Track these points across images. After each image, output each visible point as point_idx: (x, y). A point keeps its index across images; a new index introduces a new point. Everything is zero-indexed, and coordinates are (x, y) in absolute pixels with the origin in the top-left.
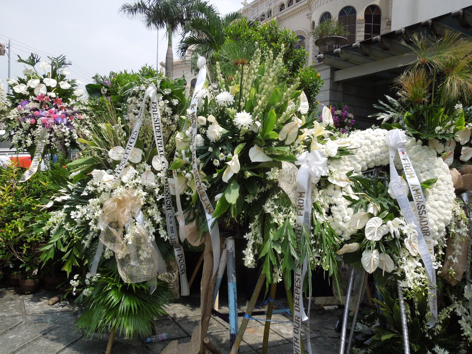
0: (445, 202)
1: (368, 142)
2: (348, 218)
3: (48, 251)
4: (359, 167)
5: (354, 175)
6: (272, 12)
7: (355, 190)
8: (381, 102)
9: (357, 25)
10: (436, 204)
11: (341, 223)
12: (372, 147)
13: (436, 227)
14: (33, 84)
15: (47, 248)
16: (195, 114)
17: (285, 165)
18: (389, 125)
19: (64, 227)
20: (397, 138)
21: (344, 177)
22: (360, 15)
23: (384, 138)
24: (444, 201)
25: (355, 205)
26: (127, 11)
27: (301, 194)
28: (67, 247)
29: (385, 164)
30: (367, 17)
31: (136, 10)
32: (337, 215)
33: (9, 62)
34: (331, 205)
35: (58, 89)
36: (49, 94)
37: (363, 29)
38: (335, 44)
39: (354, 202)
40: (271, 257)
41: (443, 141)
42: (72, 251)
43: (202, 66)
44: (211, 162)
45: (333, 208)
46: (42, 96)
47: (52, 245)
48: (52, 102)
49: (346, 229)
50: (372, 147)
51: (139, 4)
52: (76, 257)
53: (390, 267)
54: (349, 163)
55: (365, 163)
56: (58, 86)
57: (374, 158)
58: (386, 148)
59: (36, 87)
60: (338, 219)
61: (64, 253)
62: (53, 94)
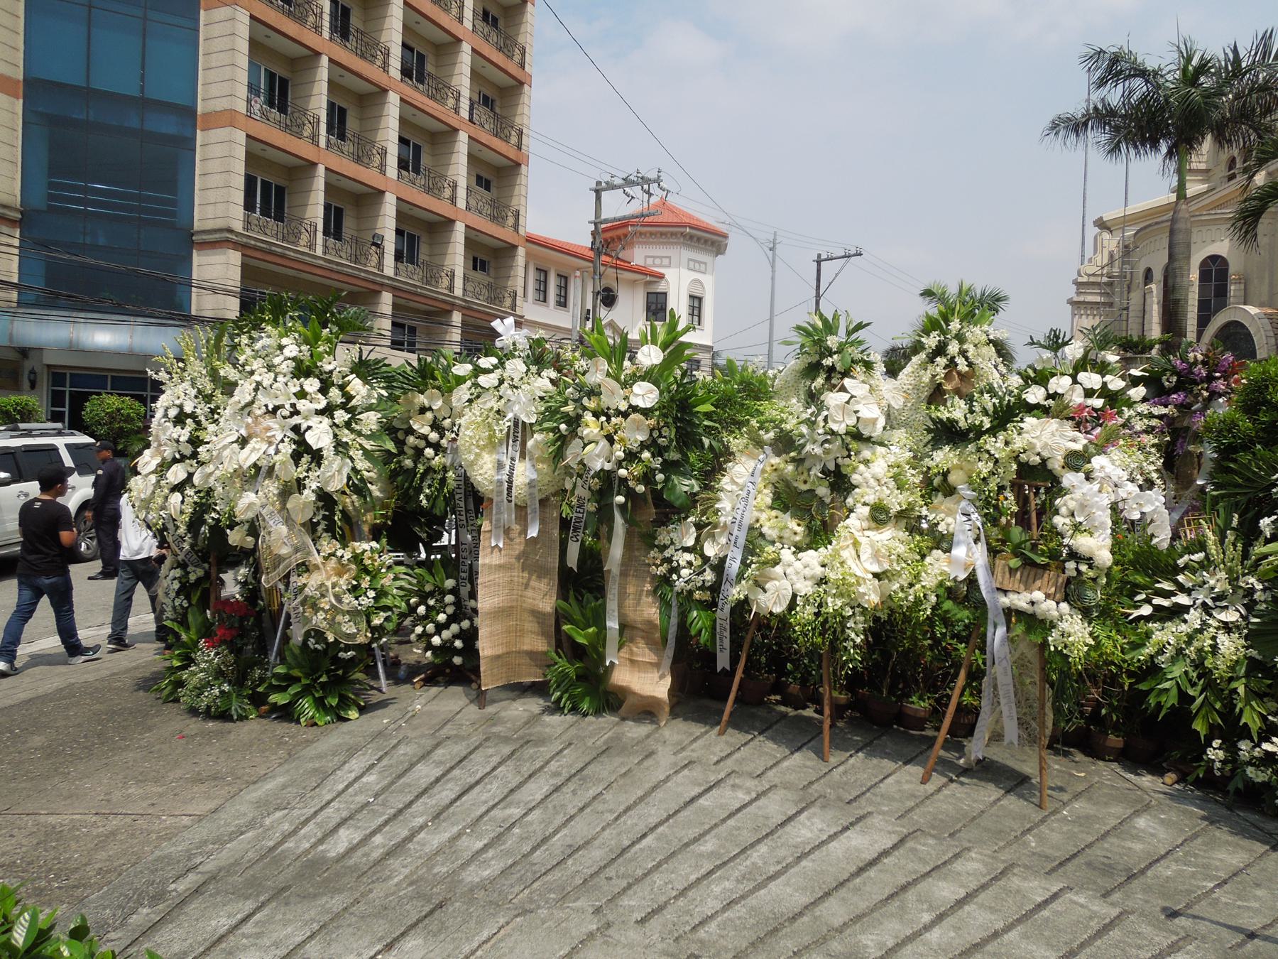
3: (1166, 690)
14: (1061, 387)
15: (1166, 685)
19: (1187, 651)
26: (1062, 133)
28: (1199, 688)
31: (1085, 124)
33: (773, 279)
35: (1104, 392)
36: (1090, 402)
42: (1206, 697)
46: (1082, 407)
47: (1174, 682)
48: (1098, 418)
51: (1096, 108)
52: (1215, 709)
56: (1105, 384)
59: (1067, 392)
61: (1193, 699)
62: (1098, 403)
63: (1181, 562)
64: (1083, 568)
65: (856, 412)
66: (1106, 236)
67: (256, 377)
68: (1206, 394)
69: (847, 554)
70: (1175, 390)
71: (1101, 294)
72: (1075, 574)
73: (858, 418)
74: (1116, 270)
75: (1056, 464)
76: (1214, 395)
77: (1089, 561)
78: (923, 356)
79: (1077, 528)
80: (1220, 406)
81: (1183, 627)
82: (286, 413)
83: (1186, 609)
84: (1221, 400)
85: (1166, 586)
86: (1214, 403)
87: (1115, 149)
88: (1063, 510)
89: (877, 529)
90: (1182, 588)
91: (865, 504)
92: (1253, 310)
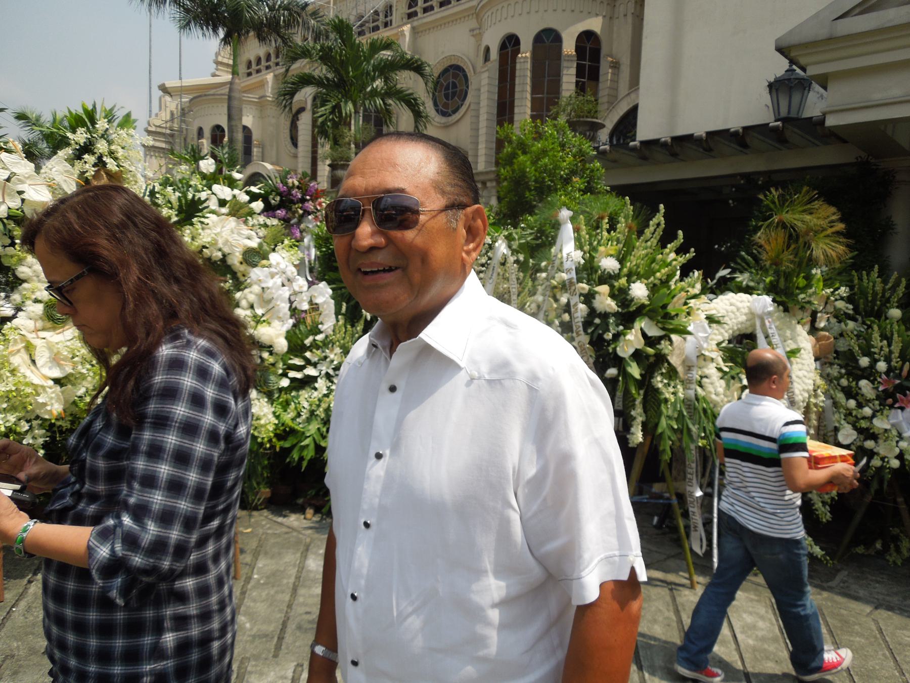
0: (807, 372)
2: (721, 390)
3: (307, 446)
4: (727, 336)
5: (724, 345)
6: (394, 9)
7: (724, 361)
8: (739, 261)
9: (564, 64)
10: (800, 374)
11: (713, 397)
12: (738, 314)
13: (800, 398)
16: (575, 280)
17: (674, 337)
18: (748, 290)
19: (318, 412)
20: (765, 306)
21: (715, 347)
22: (569, 47)
23: (748, 304)
24: (807, 371)
25: (726, 377)
27: (689, 368)
29: (749, 331)
30: (579, 49)
32: (710, 388)
34: (702, 377)
37: (573, 71)
38: (589, 130)
39: (725, 373)
40: (668, 433)
41: (802, 308)
43: (566, 223)
44: (600, 337)
45: (705, 380)
49: (718, 403)
50: (738, 314)
54: (716, 332)
55: (731, 332)
57: (739, 326)
58: (752, 315)
60: (710, 392)
63: (308, 342)
64: (266, 355)
65: (20, 193)
66: (168, 98)
68: (301, 212)
69: (19, 360)
70: (279, 207)
71: (166, 142)
72: (259, 361)
73: (23, 200)
74: (176, 126)
75: (235, 260)
76: (307, 213)
77: (270, 348)
78: (69, 151)
79: (258, 320)
80: (310, 222)
81: (316, 394)
83: (314, 379)
84: (310, 217)
85: (298, 362)
86: (305, 219)
87: (185, 26)
88: (244, 303)
89: (54, 329)
90: (308, 362)
91: (37, 301)
92: (269, 166)
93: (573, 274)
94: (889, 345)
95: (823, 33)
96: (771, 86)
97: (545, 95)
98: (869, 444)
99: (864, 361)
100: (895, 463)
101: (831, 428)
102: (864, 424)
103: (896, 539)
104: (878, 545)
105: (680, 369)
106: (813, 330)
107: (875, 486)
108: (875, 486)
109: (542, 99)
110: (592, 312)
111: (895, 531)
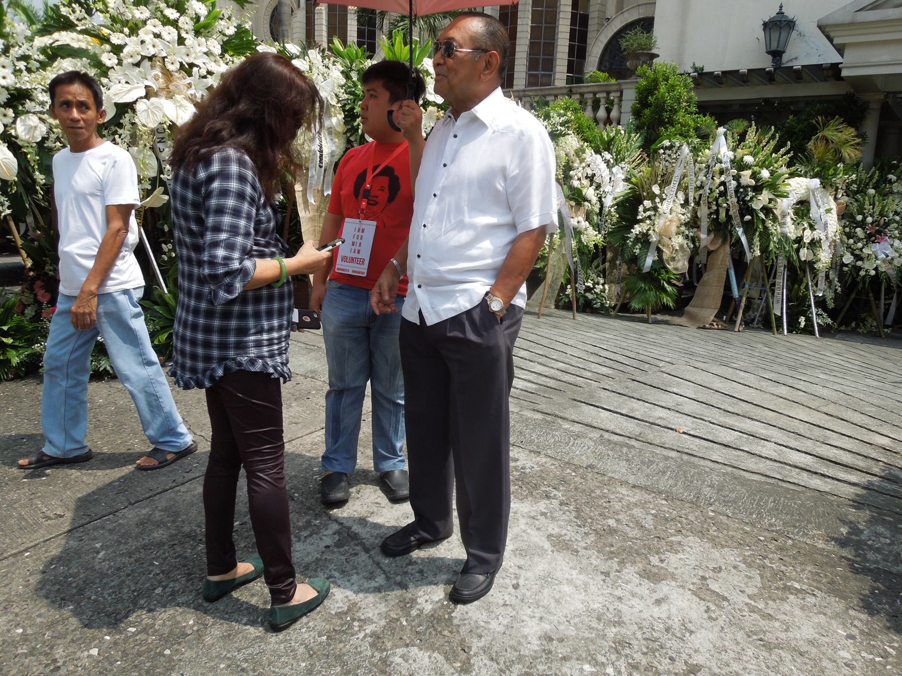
1: (799, 186)
2: (792, 231)
39: (795, 221)
53: (810, 258)
58: (808, 189)
67: (149, 27)
82: (203, 72)
88: (576, 178)
93: (729, 165)
94: (873, 209)
95: (847, 19)
96: (766, 25)
97: (544, 9)
98: (859, 263)
99: (859, 218)
100: (873, 273)
101: (839, 255)
102: (857, 252)
103: (864, 320)
104: (853, 325)
105: (779, 217)
106: (836, 199)
107: (861, 286)
108: (861, 286)
109: (542, 11)
110: (739, 186)
111: (863, 315)
